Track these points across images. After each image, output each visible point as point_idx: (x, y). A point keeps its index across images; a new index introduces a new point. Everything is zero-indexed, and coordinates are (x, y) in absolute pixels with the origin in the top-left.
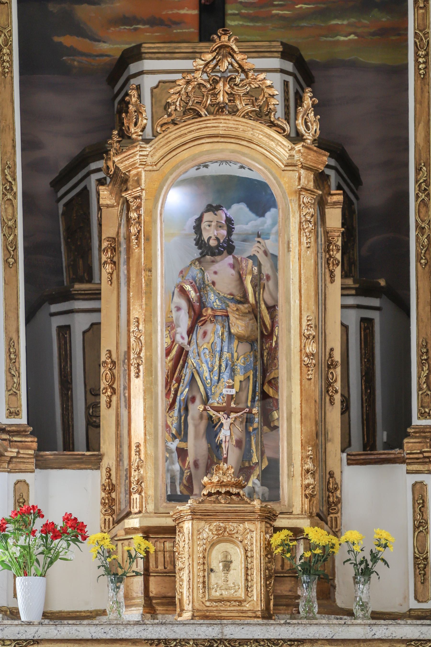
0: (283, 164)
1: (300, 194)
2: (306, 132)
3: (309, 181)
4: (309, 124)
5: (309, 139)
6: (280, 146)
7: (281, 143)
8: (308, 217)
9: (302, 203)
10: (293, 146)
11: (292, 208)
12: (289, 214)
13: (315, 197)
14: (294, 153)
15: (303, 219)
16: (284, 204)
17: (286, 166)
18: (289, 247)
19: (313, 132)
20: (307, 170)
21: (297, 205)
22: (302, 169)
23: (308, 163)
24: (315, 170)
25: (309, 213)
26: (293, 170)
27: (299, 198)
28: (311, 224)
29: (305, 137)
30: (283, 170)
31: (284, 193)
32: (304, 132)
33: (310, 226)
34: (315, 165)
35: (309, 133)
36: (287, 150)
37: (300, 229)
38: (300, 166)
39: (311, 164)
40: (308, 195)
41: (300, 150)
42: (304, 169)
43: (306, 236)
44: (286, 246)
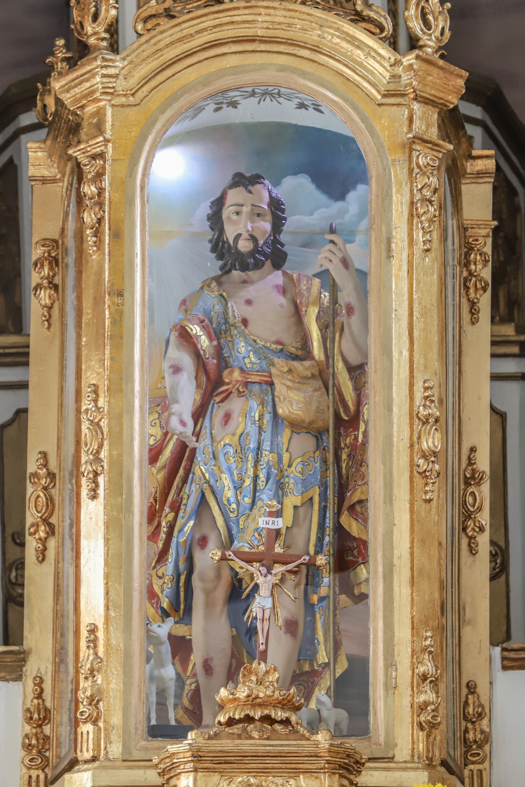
0: (379, 92)
1: (411, 150)
2: (424, 33)
3: (428, 126)
4: (430, 17)
5: (430, 47)
6: (373, 58)
7: (376, 51)
8: (427, 193)
9: (416, 167)
10: (399, 57)
11: (396, 176)
12: (390, 187)
13: (440, 155)
14: (399, 70)
15: (418, 197)
16: (381, 169)
17: (384, 96)
18: (389, 249)
19: (438, 33)
20: (426, 103)
21: (406, 171)
22: (415, 103)
23: (428, 89)
24: (441, 104)
25: (430, 186)
26: (398, 105)
27: (410, 156)
28: (432, 205)
29: (421, 43)
30: (379, 105)
31: (380, 146)
32: (420, 33)
33: (431, 209)
34: (441, 95)
35: (430, 35)
36: (386, 65)
37: (411, 215)
38: (412, 96)
39: (433, 92)
40: (427, 151)
41: (411, 65)
42: (419, 102)
43: (423, 228)
44: (383, 247)
